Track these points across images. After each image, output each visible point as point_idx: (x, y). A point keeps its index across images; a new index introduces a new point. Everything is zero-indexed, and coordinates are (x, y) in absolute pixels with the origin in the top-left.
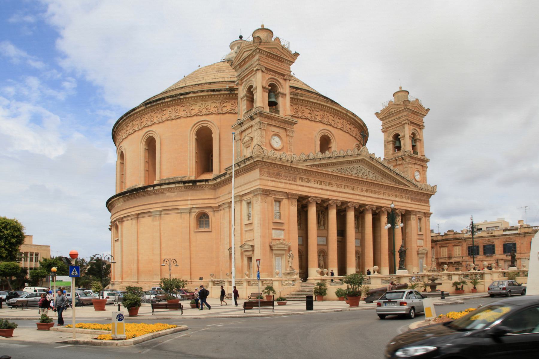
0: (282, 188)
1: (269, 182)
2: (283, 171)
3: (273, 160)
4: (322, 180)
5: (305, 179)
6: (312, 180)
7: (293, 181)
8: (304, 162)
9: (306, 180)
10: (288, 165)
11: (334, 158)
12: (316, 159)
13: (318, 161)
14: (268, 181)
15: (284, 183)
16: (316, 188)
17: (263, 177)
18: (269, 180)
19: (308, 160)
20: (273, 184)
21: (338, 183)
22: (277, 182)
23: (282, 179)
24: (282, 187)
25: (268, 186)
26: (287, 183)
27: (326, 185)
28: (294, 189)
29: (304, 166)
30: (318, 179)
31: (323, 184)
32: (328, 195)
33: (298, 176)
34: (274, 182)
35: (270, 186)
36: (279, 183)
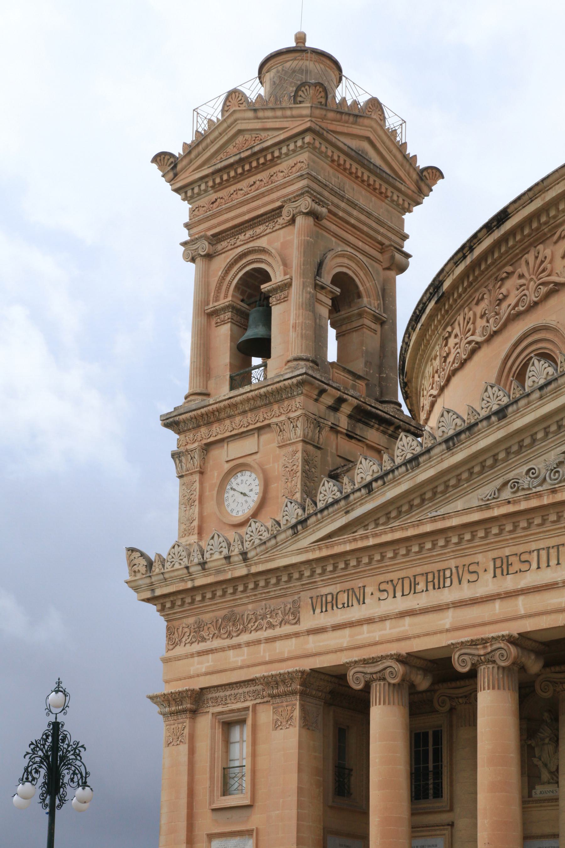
0: (241, 668)
1: (196, 659)
2: (245, 601)
3: (182, 580)
4: (419, 570)
5: (335, 598)
6: (368, 590)
7: (287, 622)
8: (295, 534)
9: (343, 598)
10: (242, 571)
11: (444, 446)
12: (347, 497)
13: (361, 501)
14: (191, 660)
15: (248, 644)
16: (383, 619)
17: (180, 650)
18: (192, 655)
19: (313, 519)
20: (209, 662)
21: (507, 552)
22: (223, 649)
23: (245, 630)
24: (239, 664)
25: (191, 677)
26: (258, 642)
27: (439, 587)
28: (286, 655)
29: (305, 550)
30: (394, 576)
31: (421, 586)
32: (447, 631)
33: (305, 596)
34: (210, 656)
35: (198, 676)
36: (231, 653)
